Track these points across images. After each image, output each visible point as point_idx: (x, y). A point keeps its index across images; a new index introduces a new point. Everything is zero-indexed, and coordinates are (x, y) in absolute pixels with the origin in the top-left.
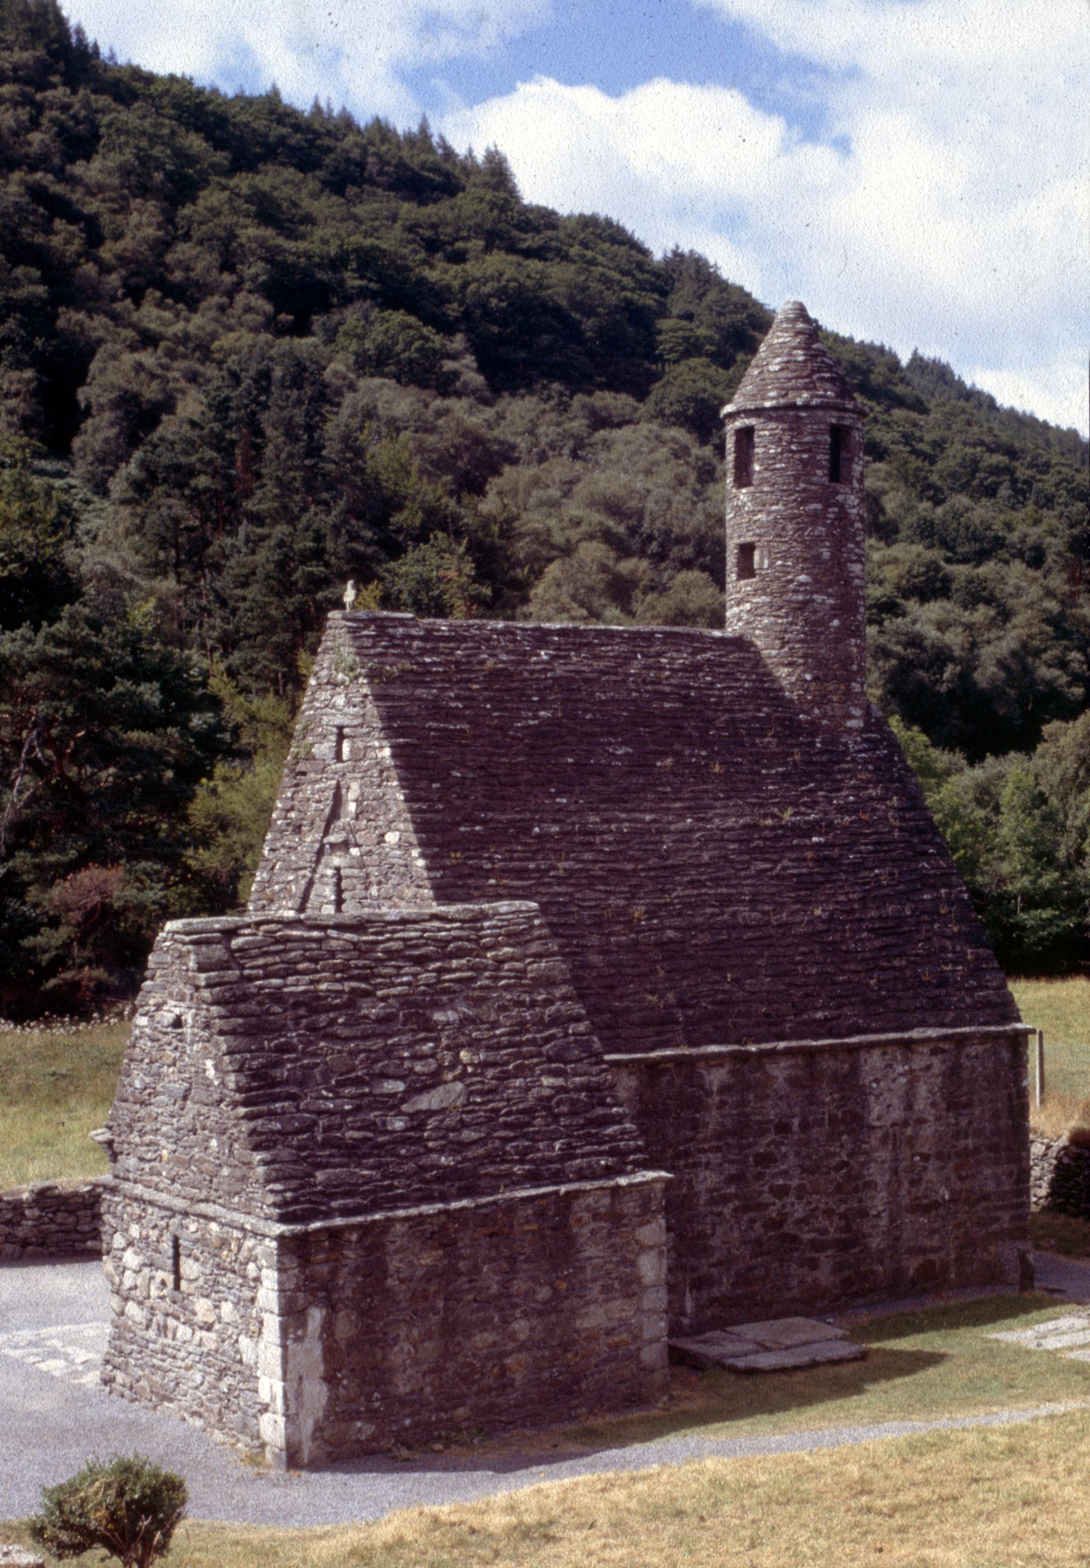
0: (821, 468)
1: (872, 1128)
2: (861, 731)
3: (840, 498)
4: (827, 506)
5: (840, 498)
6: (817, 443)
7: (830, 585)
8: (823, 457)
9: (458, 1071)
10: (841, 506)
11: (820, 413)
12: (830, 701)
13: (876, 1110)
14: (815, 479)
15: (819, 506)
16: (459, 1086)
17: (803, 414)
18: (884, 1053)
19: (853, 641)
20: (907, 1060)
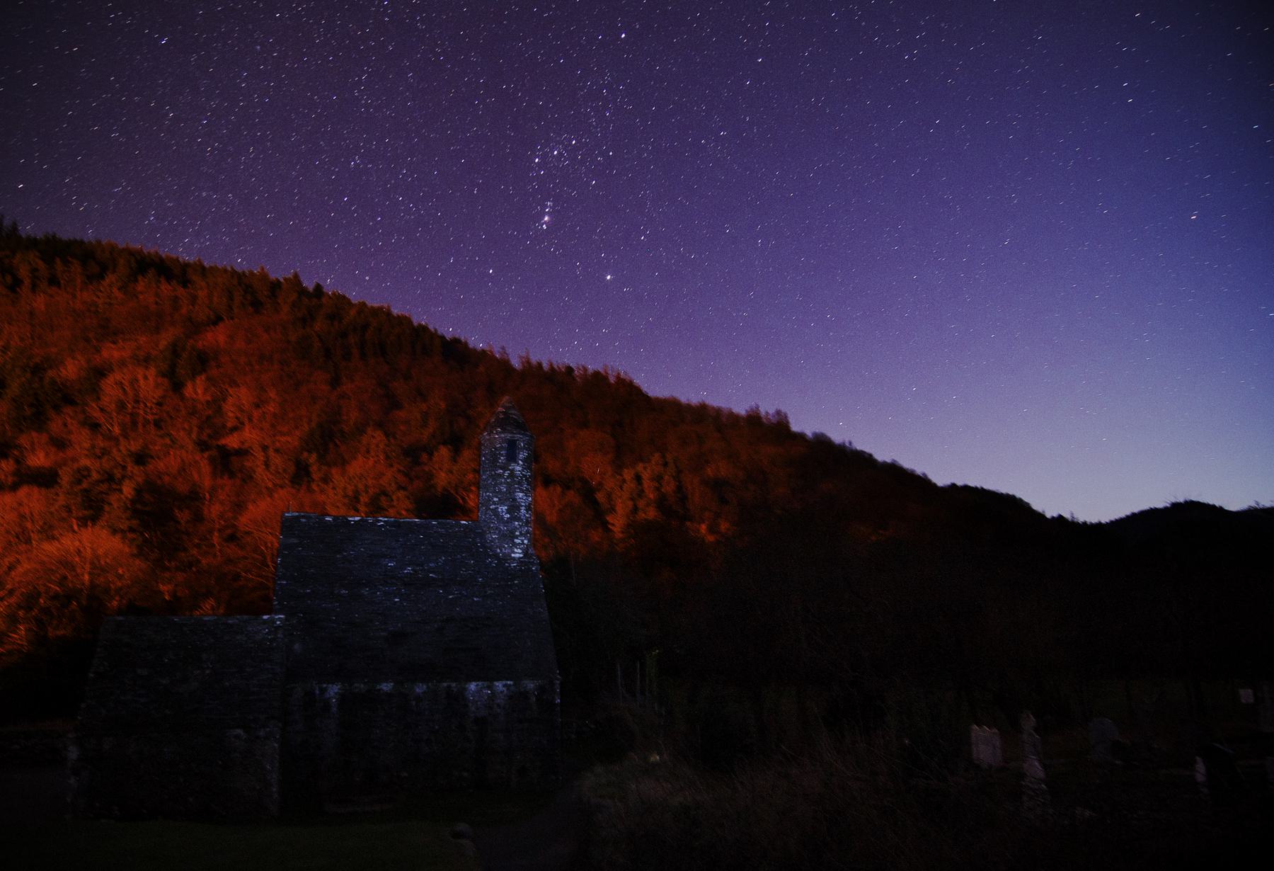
2: (520, 558)
10: (512, 471)
14: (500, 461)
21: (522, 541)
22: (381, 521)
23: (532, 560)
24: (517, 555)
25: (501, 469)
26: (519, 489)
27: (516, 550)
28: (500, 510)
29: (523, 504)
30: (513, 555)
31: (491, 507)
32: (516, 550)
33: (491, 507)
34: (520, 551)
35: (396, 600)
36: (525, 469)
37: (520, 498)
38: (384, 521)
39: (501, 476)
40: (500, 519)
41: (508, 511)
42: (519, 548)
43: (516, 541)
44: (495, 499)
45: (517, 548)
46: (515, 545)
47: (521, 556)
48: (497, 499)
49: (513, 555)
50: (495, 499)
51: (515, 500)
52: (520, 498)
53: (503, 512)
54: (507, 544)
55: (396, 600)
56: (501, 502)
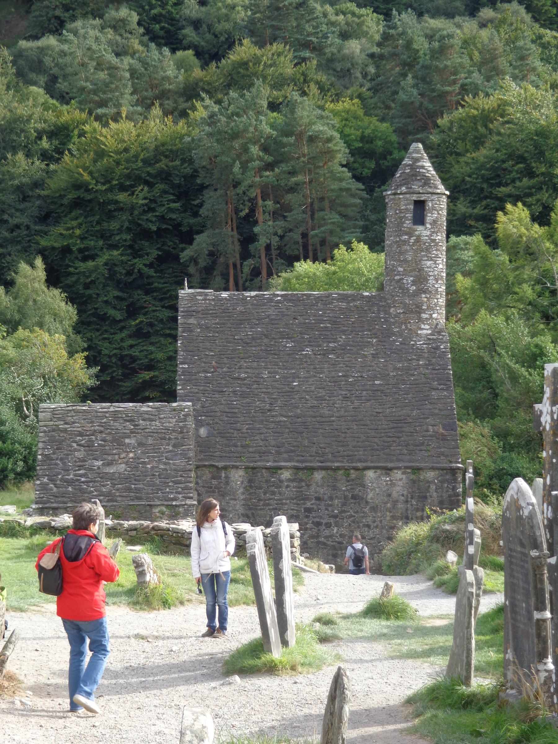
0: (409, 220)
1: (367, 502)
3: (417, 233)
4: (410, 237)
5: (417, 233)
6: (407, 209)
7: (411, 271)
8: (410, 215)
9: (125, 460)
10: (419, 237)
11: (408, 196)
12: (410, 323)
13: (371, 495)
14: (405, 225)
15: (406, 237)
16: (123, 465)
17: (401, 196)
18: (375, 472)
19: (424, 296)
20: (388, 475)
21: (431, 315)
22: (278, 296)
23: (441, 337)
24: (425, 332)
25: (406, 234)
26: (428, 257)
27: (423, 326)
28: (405, 281)
29: (431, 274)
30: (419, 332)
31: (396, 278)
32: (423, 326)
33: (396, 278)
34: (428, 327)
35: (295, 384)
36: (433, 232)
37: (428, 267)
38: (282, 296)
39: (405, 242)
40: (404, 290)
41: (414, 283)
42: (428, 324)
43: (424, 316)
44: (401, 269)
45: (424, 324)
46: (420, 320)
47: (429, 332)
48: (402, 269)
49: (419, 332)
50: (401, 269)
51: (421, 270)
52: (428, 267)
53: (408, 284)
54: (412, 320)
55: (295, 384)
56: (406, 273)
